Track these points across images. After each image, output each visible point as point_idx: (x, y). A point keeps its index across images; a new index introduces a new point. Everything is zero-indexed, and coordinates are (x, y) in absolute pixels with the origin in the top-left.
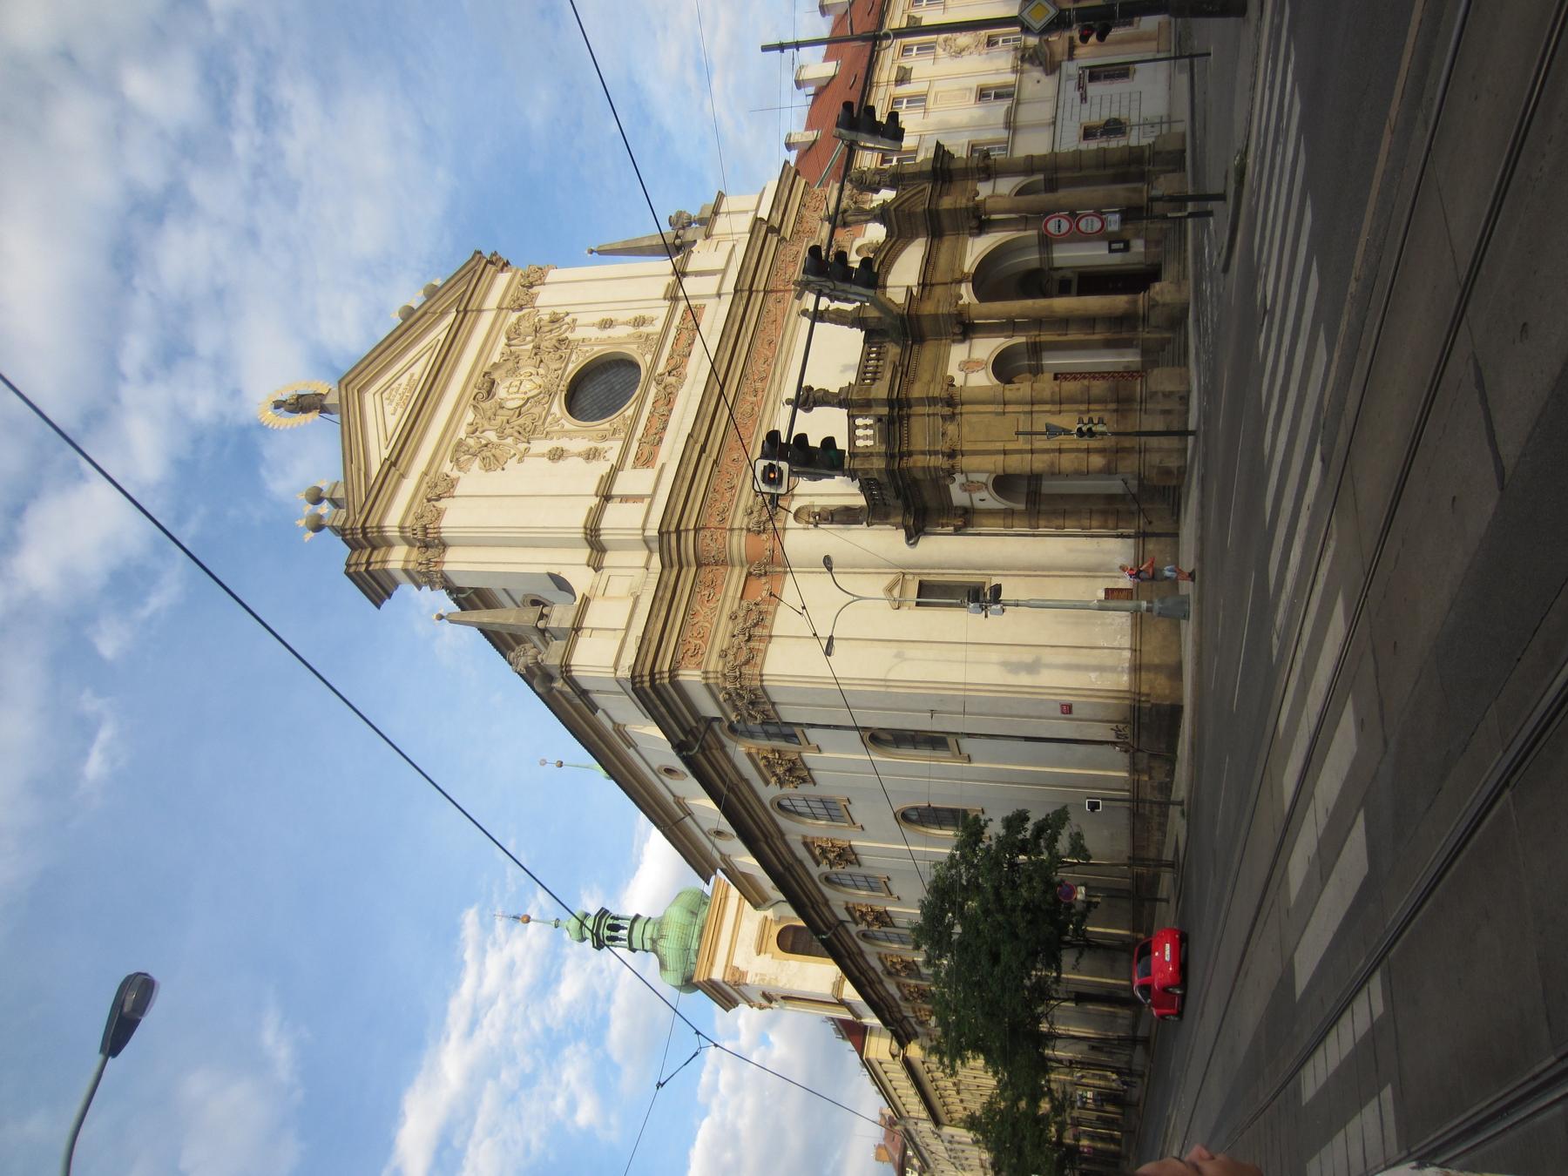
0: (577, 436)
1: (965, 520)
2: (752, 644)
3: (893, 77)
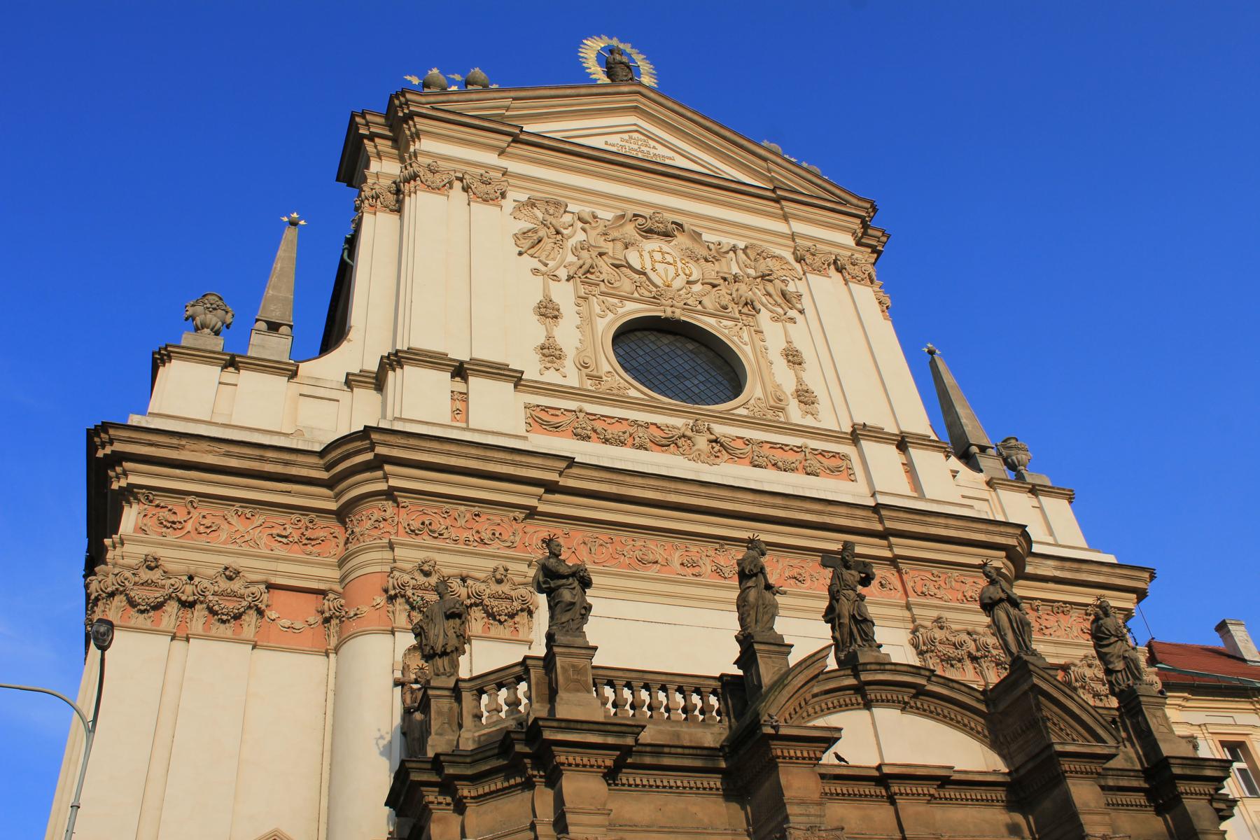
0: (587, 332)
2: (172, 607)
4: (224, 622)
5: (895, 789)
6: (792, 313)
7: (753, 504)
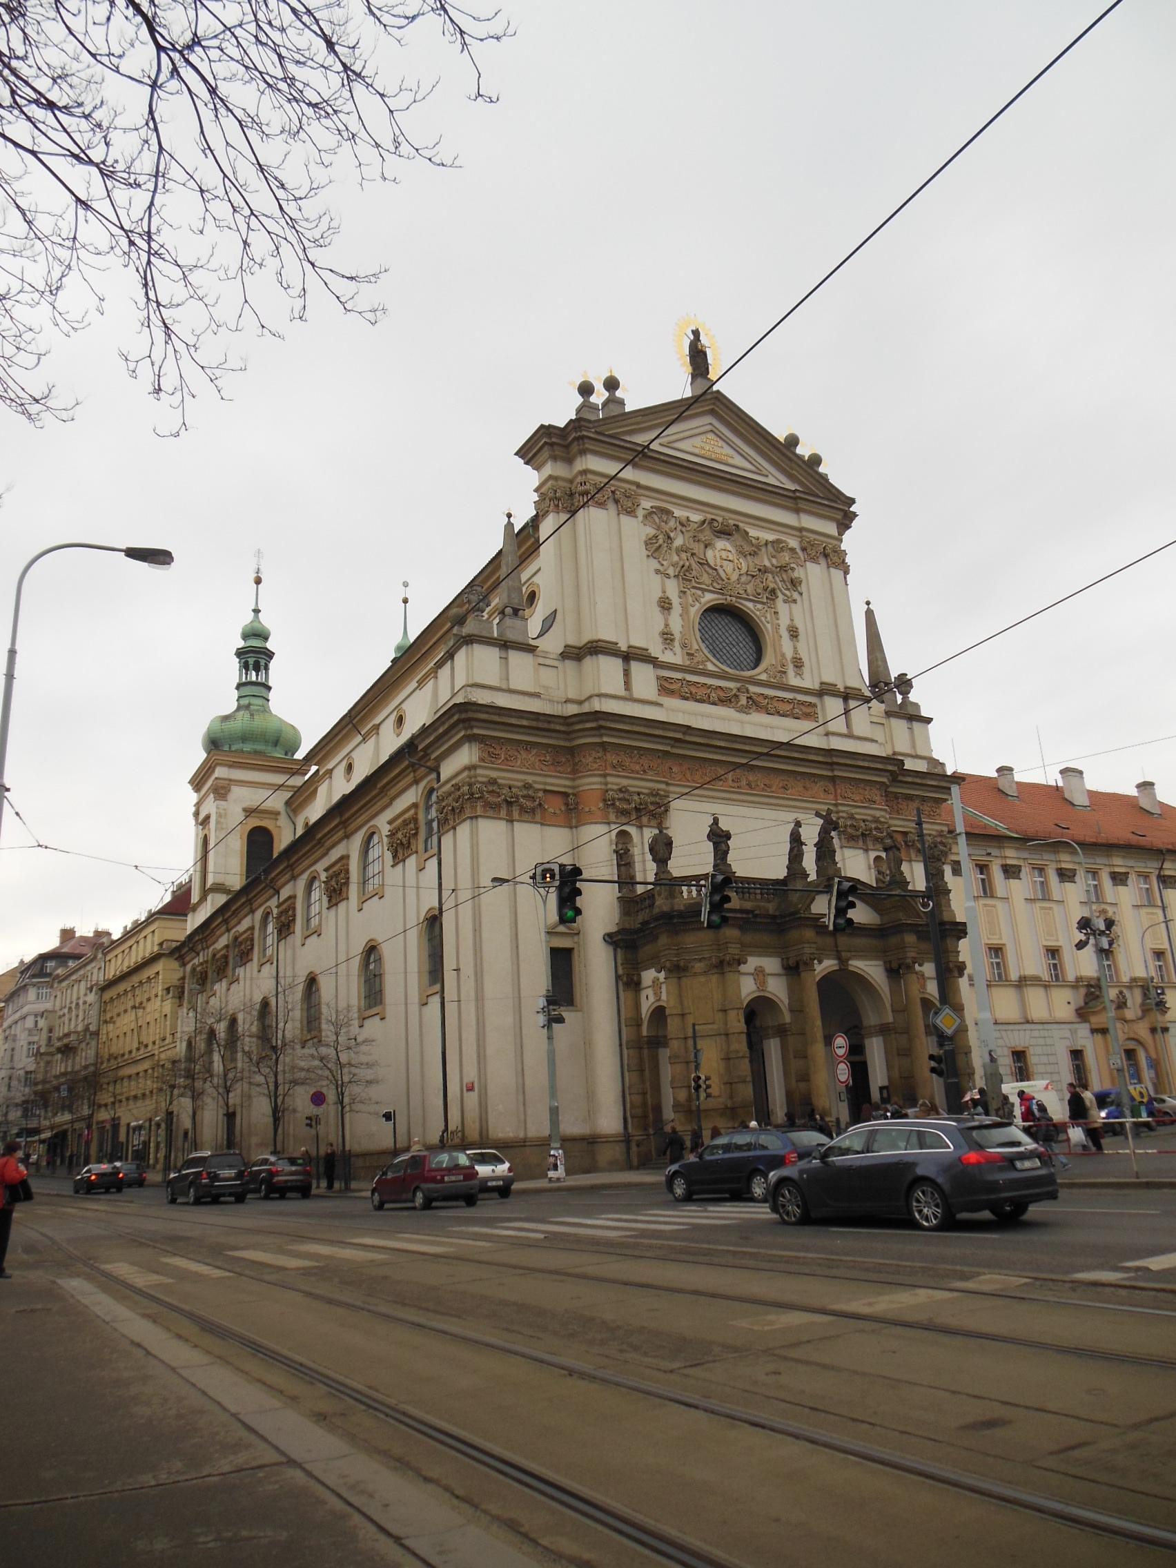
1: (628, 982)
2: (504, 806)
3: (1064, 865)
6: (796, 595)
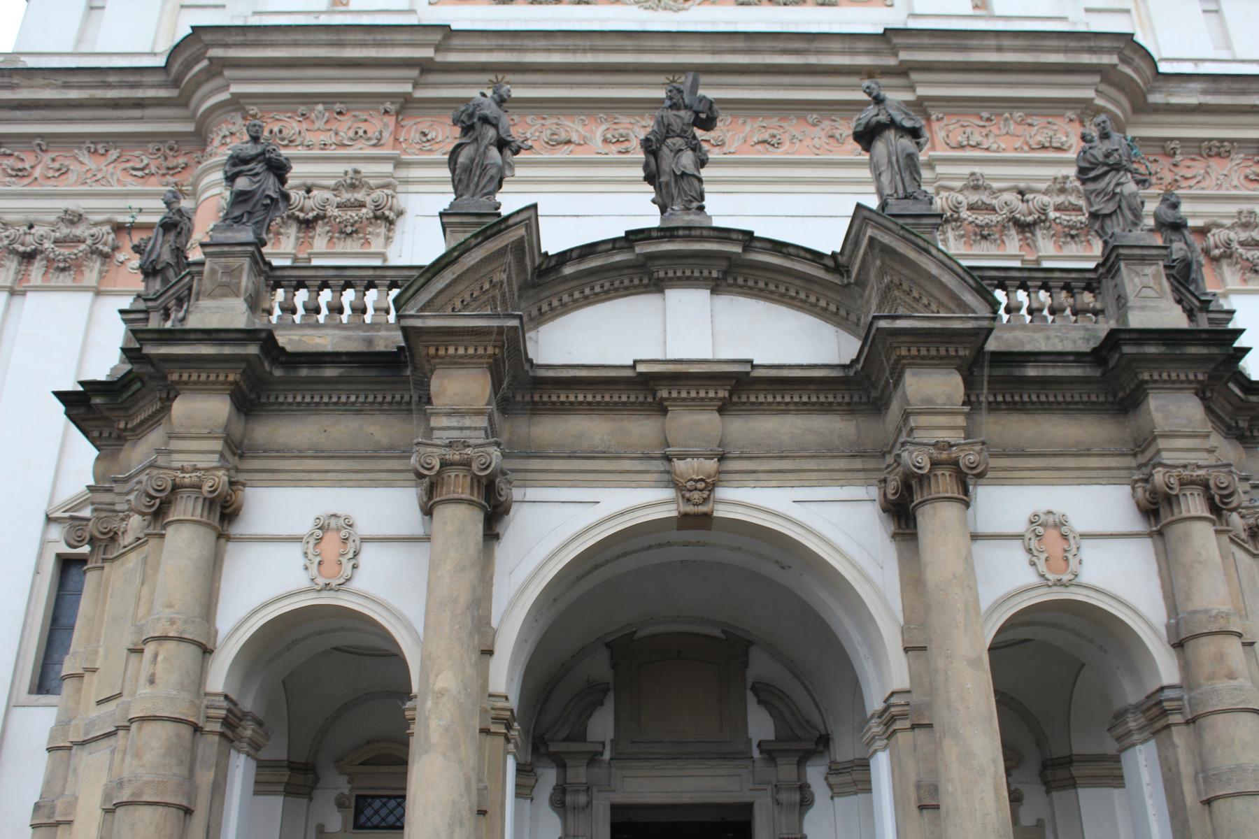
4: (63, 270)
5: (664, 393)
7: (703, 51)
